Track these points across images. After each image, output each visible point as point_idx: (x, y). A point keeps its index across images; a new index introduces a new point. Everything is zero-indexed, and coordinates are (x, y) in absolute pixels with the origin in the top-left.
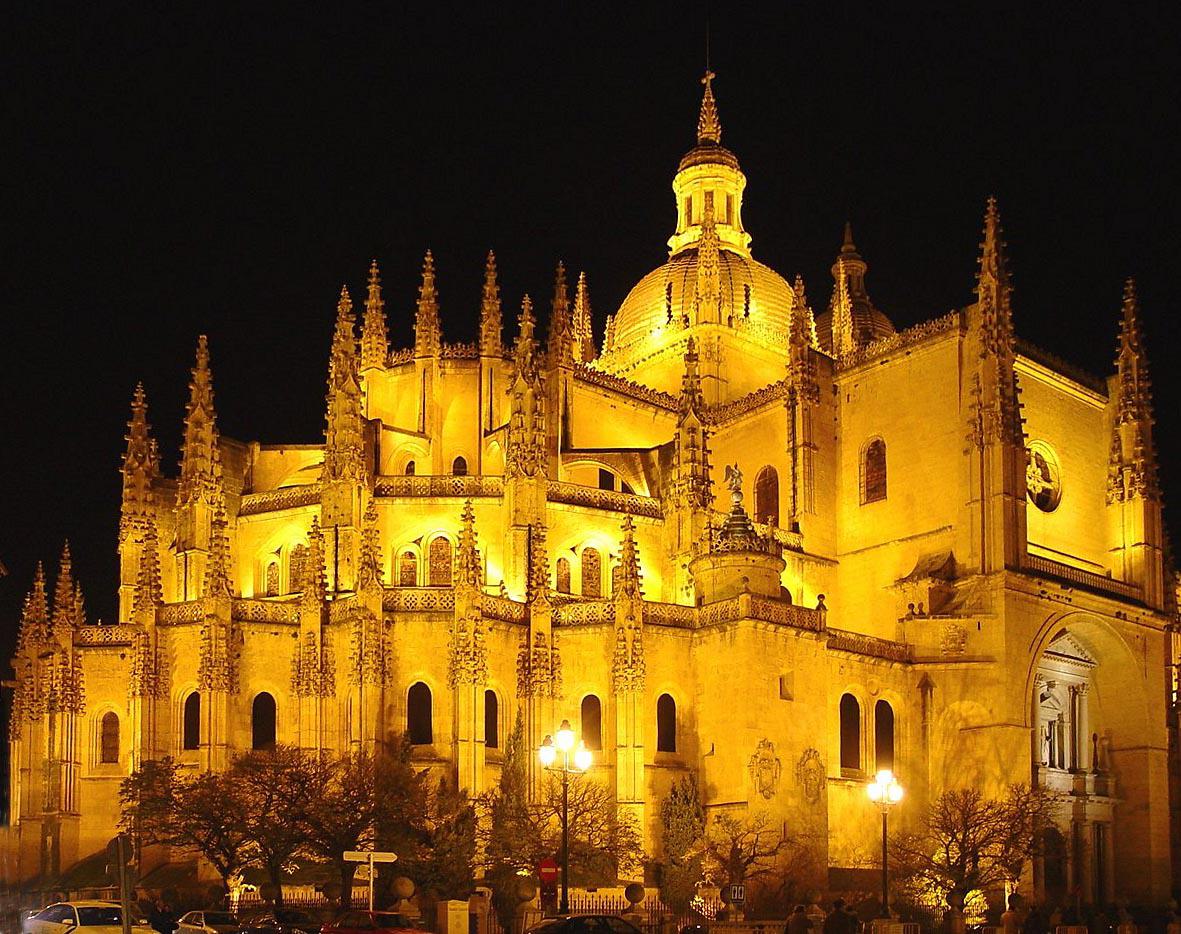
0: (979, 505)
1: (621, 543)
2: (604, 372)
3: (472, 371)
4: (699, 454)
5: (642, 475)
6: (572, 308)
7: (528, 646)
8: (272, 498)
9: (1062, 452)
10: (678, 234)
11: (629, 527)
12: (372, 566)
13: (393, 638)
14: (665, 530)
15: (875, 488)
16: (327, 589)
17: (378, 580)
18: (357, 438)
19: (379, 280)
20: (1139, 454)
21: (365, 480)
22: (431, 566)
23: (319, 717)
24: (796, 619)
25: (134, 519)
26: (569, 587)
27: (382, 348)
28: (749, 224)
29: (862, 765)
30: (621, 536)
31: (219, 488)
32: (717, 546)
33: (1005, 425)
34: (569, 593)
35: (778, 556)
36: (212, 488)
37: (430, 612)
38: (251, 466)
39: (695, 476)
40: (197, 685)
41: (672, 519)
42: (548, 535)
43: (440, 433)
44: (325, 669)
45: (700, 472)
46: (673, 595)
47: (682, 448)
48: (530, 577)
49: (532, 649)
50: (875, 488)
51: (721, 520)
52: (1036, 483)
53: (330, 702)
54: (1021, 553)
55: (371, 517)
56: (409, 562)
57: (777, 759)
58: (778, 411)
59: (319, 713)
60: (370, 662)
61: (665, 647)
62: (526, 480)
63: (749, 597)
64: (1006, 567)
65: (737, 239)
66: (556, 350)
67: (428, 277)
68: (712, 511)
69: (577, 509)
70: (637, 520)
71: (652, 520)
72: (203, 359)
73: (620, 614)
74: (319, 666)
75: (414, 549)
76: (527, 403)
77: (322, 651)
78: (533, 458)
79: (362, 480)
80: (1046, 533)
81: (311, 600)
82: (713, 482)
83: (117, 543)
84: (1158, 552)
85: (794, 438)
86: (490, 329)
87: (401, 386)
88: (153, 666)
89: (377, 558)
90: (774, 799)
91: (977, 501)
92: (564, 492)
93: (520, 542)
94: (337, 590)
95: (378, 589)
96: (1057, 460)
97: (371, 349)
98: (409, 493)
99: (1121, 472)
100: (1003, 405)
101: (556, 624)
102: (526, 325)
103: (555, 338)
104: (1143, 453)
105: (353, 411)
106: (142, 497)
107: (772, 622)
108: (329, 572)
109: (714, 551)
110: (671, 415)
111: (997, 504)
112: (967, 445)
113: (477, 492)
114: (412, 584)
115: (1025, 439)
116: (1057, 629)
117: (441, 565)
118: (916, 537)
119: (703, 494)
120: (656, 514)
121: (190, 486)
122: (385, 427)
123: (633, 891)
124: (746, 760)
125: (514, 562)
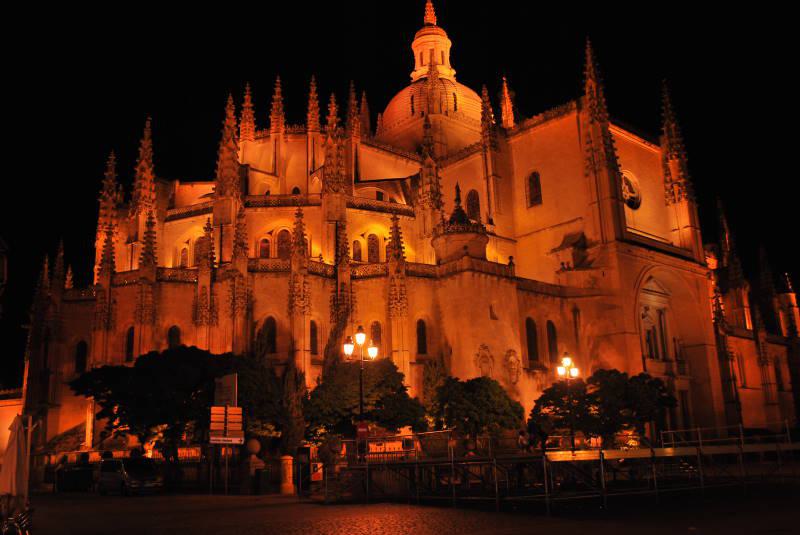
0: (596, 205)
4: (434, 180)
5: (401, 193)
6: (359, 105)
9: (639, 176)
11: (395, 219)
12: (241, 245)
15: (535, 199)
18: (235, 174)
28: (454, 63)
29: (541, 360)
31: (154, 206)
33: (609, 160)
37: (277, 271)
38: (174, 195)
40: (133, 321)
41: (419, 218)
42: (347, 226)
44: (213, 309)
45: (435, 189)
48: (337, 250)
49: (339, 293)
50: (535, 199)
51: (447, 217)
53: (215, 330)
55: (240, 216)
56: (265, 245)
58: (478, 158)
60: (240, 303)
64: (617, 239)
65: (447, 72)
67: (278, 90)
68: (443, 211)
69: (365, 212)
72: (147, 133)
73: (392, 270)
75: (268, 237)
76: (334, 151)
79: (237, 197)
80: (641, 221)
83: (94, 241)
84: (699, 231)
86: (313, 117)
92: (357, 202)
94: (221, 262)
98: (267, 205)
99: (672, 187)
100: (606, 150)
101: (353, 278)
102: (333, 109)
104: (684, 177)
106: (110, 214)
108: (217, 251)
110: (416, 163)
112: (587, 172)
113: (307, 204)
114: (267, 257)
116: (647, 276)
117: (284, 246)
120: (411, 214)
121: (137, 204)
122: (253, 169)
123: (407, 444)
124: (472, 358)
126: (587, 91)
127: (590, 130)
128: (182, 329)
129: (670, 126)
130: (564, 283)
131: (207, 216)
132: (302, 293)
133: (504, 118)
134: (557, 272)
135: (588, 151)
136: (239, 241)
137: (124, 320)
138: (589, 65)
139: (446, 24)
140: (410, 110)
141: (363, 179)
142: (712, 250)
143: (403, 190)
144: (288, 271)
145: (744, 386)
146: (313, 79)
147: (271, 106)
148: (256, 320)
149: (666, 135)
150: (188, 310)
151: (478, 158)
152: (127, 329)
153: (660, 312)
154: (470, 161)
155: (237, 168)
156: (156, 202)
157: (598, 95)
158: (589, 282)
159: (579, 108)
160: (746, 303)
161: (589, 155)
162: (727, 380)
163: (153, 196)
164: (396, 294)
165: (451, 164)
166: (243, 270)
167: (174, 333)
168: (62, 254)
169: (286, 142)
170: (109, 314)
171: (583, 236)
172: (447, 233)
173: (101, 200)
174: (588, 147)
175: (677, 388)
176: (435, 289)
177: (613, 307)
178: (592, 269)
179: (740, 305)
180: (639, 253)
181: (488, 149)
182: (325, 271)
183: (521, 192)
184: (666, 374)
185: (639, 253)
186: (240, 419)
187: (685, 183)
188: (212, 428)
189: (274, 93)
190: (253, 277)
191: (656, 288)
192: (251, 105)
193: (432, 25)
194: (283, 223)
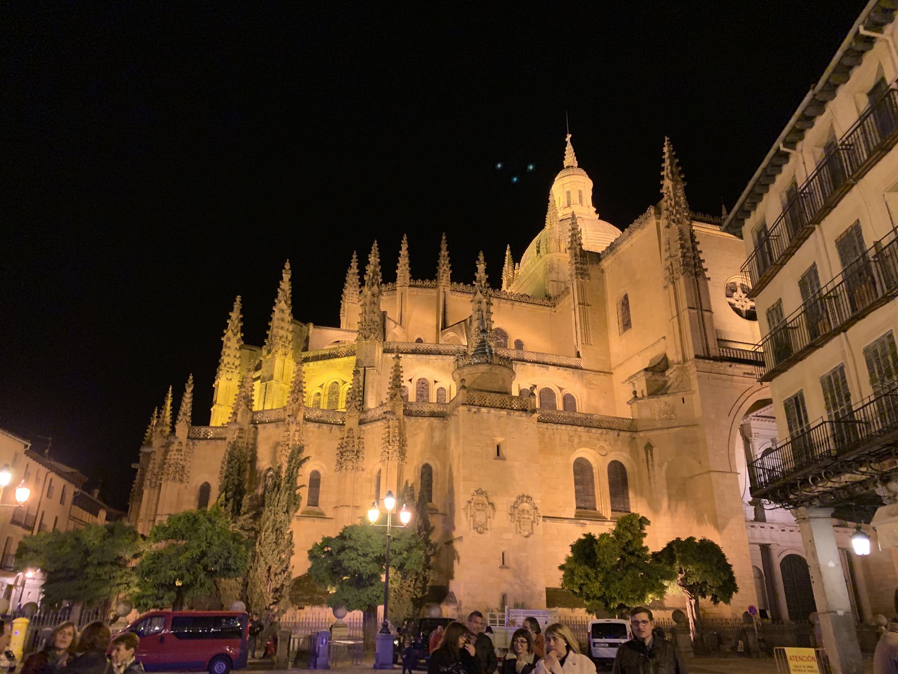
0: (676, 319)
15: (627, 324)
27: (355, 293)
33: (686, 265)
49: (345, 440)
50: (627, 324)
52: (744, 304)
62: (364, 342)
63: (465, 392)
64: (697, 357)
90: (488, 534)
112: (666, 283)
130: (636, 417)
143: (467, 333)
156: (239, 368)
157: (675, 195)
158: (666, 413)
161: (668, 263)
171: (665, 358)
174: (668, 254)
192: (357, 271)
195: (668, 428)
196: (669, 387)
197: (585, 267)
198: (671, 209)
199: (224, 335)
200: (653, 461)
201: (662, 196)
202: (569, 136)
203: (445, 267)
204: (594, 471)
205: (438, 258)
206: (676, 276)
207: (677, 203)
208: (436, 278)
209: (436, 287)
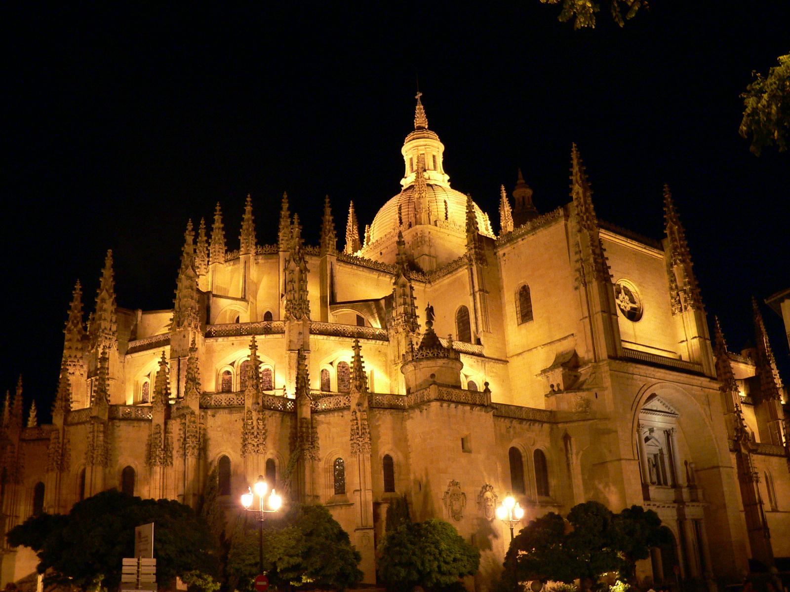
0: (587, 320)
1: (353, 357)
2: (363, 258)
3: (274, 260)
4: (408, 300)
5: (376, 315)
7: (296, 428)
8: (146, 342)
9: (640, 285)
10: (406, 178)
11: (357, 348)
13: (206, 426)
14: (389, 349)
15: (526, 315)
16: (170, 397)
17: (196, 389)
18: (193, 303)
19: (221, 213)
20: (687, 283)
21: (199, 328)
22: (241, 379)
23: (162, 479)
24: (470, 399)
25: (69, 360)
26: (329, 387)
27: (221, 251)
28: (447, 168)
30: (353, 353)
32: (416, 355)
33: (598, 271)
34: (329, 391)
35: (458, 359)
36: (110, 339)
37: (230, 408)
38: (136, 324)
39: (406, 313)
43: (255, 297)
44: (167, 448)
45: (409, 310)
46: (397, 388)
47: (397, 296)
50: (526, 315)
53: (170, 471)
54: (618, 347)
57: (463, 493)
58: (464, 272)
59: (162, 477)
61: (385, 422)
62: (296, 322)
64: (610, 357)
65: (440, 178)
66: (326, 245)
67: (248, 208)
69: (332, 338)
70: (362, 342)
71: (381, 342)
74: (162, 447)
75: (230, 369)
77: (165, 436)
78: (301, 308)
79: (196, 328)
81: (159, 404)
82: (418, 317)
85: (473, 287)
87: (233, 272)
88: (60, 451)
89: (196, 375)
91: (586, 317)
93: (293, 361)
94: (178, 397)
95: (197, 395)
96: (637, 289)
97: (215, 251)
99: (678, 295)
101: (314, 412)
103: (325, 238)
104: (689, 283)
105: (191, 287)
106: (75, 347)
107: (453, 402)
109: (415, 358)
111: (599, 319)
112: (577, 284)
113: (267, 331)
114: (229, 391)
115: (611, 279)
118: (553, 342)
119: (412, 324)
122: (214, 296)
125: (290, 373)
126: (574, 197)
127: (578, 239)
128: (135, 470)
129: (673, 228)
130: (554, 408)
131: (161, 349)
132: (255, 431)
133: (502, 224)
134: (546, 396)
135: (577, 261)
136: (190, 376)
137: (77, 462)
138: (576, 169)
139: (436, 126)
140: (398, 221)
141: (339, 300)
142: (749, 355)
144: (241, 407)
145: (775, 510)
146: (285, 196)
147: (241, 227)
148: (210, 460)
149: (669, 238)
150: (142, 449)
151: (464, 272)
152: (80, 471)
153: (668, 433)
154: (458, 275)
155: (196, 296)
157: (585, 202)
158: (581, 406)
159: (567, 216)
160: (780, 415)
161: (578, 265)
162: (751, 503)
163: (114, 328)
164: (358, 428)
165: (440, 277)
166: (195, 407)
167: (128, 475)
168: (21, 391)
169: (257, 263)
170: (63, 455)
171: (575, 355)
172: (416, 360)
173: (65, 332)
174: (578, 257)
175: (688, 517)
176: (403, 420)
177: (608, 432)
178: (584, 390)
179: (775, 418)
180: (636, 371)
181: (474, 263)
182: (284, 406)
183: (511, 309)
184: (675, 502)
185: (636, 371)
186: (153, 570)
187: (692, 290)
188: (123, 580)
189: (244, 212)
190: (206, 413)
191: (661, 407)
192: (222, 226)
193: (424, 128)
194: (240, 353)
195: (584, 420)
196: (584, 382)
197: (483, 252)
198: (582, 214)
199: (97, 295)
200: (571, 450)
201: (571, 199)
202: (419, 95)
203: (331, 234)
204: (523, 459)
205: (322, 222)
206: (587, 279)
207: (587, 210)
208: (320, 247)
209: (318, 255)
